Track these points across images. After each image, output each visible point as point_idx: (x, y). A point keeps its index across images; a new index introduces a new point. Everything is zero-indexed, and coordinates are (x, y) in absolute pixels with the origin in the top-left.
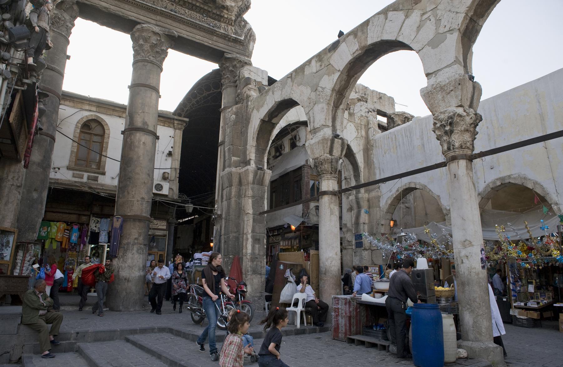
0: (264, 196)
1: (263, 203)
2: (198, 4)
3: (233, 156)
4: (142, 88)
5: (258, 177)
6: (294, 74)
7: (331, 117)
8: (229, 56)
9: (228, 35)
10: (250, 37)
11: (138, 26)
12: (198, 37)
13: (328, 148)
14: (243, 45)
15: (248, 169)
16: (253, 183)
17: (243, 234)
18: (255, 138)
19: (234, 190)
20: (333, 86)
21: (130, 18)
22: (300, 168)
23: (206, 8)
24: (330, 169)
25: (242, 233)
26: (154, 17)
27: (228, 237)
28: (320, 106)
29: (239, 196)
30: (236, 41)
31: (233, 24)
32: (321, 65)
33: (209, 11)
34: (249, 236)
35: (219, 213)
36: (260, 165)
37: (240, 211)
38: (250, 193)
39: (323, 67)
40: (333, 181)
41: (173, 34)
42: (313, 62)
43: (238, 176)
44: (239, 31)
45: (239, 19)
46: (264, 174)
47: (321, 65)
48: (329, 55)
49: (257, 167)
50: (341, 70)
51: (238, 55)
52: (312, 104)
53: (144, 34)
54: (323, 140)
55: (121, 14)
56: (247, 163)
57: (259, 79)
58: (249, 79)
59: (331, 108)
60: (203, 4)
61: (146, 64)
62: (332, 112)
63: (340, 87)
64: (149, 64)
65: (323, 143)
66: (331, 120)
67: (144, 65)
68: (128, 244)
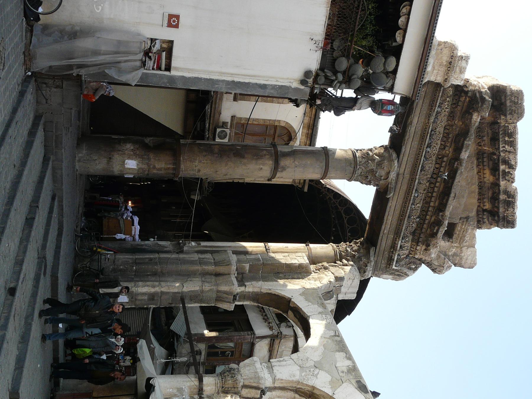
0: (204, 303)
1: (195, 302)
2: (428, 217)
3: (250, 265)
4: (324, 164)
5: (225, 295)
6: (338, 339)
7: (285, 385)
9: (396, 250)
10: (398, 275)
11: (394, 155)
12: (390, 218)
13: (249, 384)
14: (386, 267)
15: (233, 284)
16: (218, 291)
17: (160, 281)
18: (270, 292)
19: (211, 268)
20: (318, 387)
21: (403, 148)
22: (250, 329)
23: (425, 226)
24: (227, 386)
25: (161, 279)
26: (408, 171)
27: (156, 263)
28: (298, 373)
29: (205, 274)
30: (390, 260)
31: (411, 256)
32: (343, 372)
33: (421, 230)
34: (157, 289)
35: (185, 248)
36: (240, 297)
37: (187, 276)
38: (207, 287)
39: (341, 374)
40: (214, 389)
41: (388, 192)
42: (348, 363)
43: (226, 272)
44: (403, 263)
45: (419, 262)
46: (230, 302)
47: (343, 372)
48: (354, 381)
49: (237, 294)
50: (334, 396)
51: (373, 263)
52: (300, 362)
53: (386, 163)
54: (259, 377)
55: (406, 138)
56: (241, 282)
57: (343, 289)
59: (294, 386)
60: (429, 222)
61: (353, 166)
62: (290, 386)
63: (317, 395)
64: (352, 169)
65: (255, 378)
66: (281, 385)
67: (351, 164)
68: (149, 159)
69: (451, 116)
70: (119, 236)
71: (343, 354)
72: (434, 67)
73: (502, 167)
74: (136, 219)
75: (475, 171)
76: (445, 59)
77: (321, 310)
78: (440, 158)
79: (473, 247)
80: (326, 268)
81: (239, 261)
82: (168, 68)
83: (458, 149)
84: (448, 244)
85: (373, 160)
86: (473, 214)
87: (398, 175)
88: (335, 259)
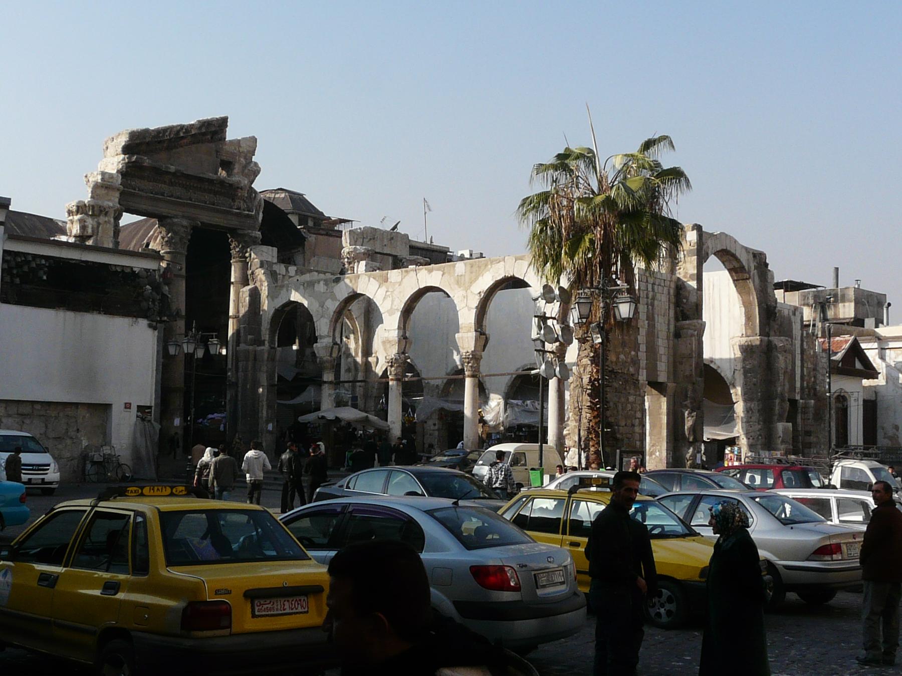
8: (240, 232)
11: (169, 221)
19: (250, 364)
30: (248, 216)
34: (265, 403)
35: (233, 380)
38: (264, 368)
42: (322, 283)
53: (175, 228)
56: (262, 343)
57: (269, 260)
70: (222, 428)
71: (316, 285)
72: (109, 200)
73: (182, 134)
74: (210, 416)
75: (181, 149)
76: (103, 192)
77: (285, 290)
78: (172, 184)
79: (239, 141)
80: (253, 273)
81: (245, 343)
82: (150, 407)
83: (168, 173)
84: (237, 166)
85: (172, 238)
86: (213, 145)
87: (183, 217)
88: (245, 265)
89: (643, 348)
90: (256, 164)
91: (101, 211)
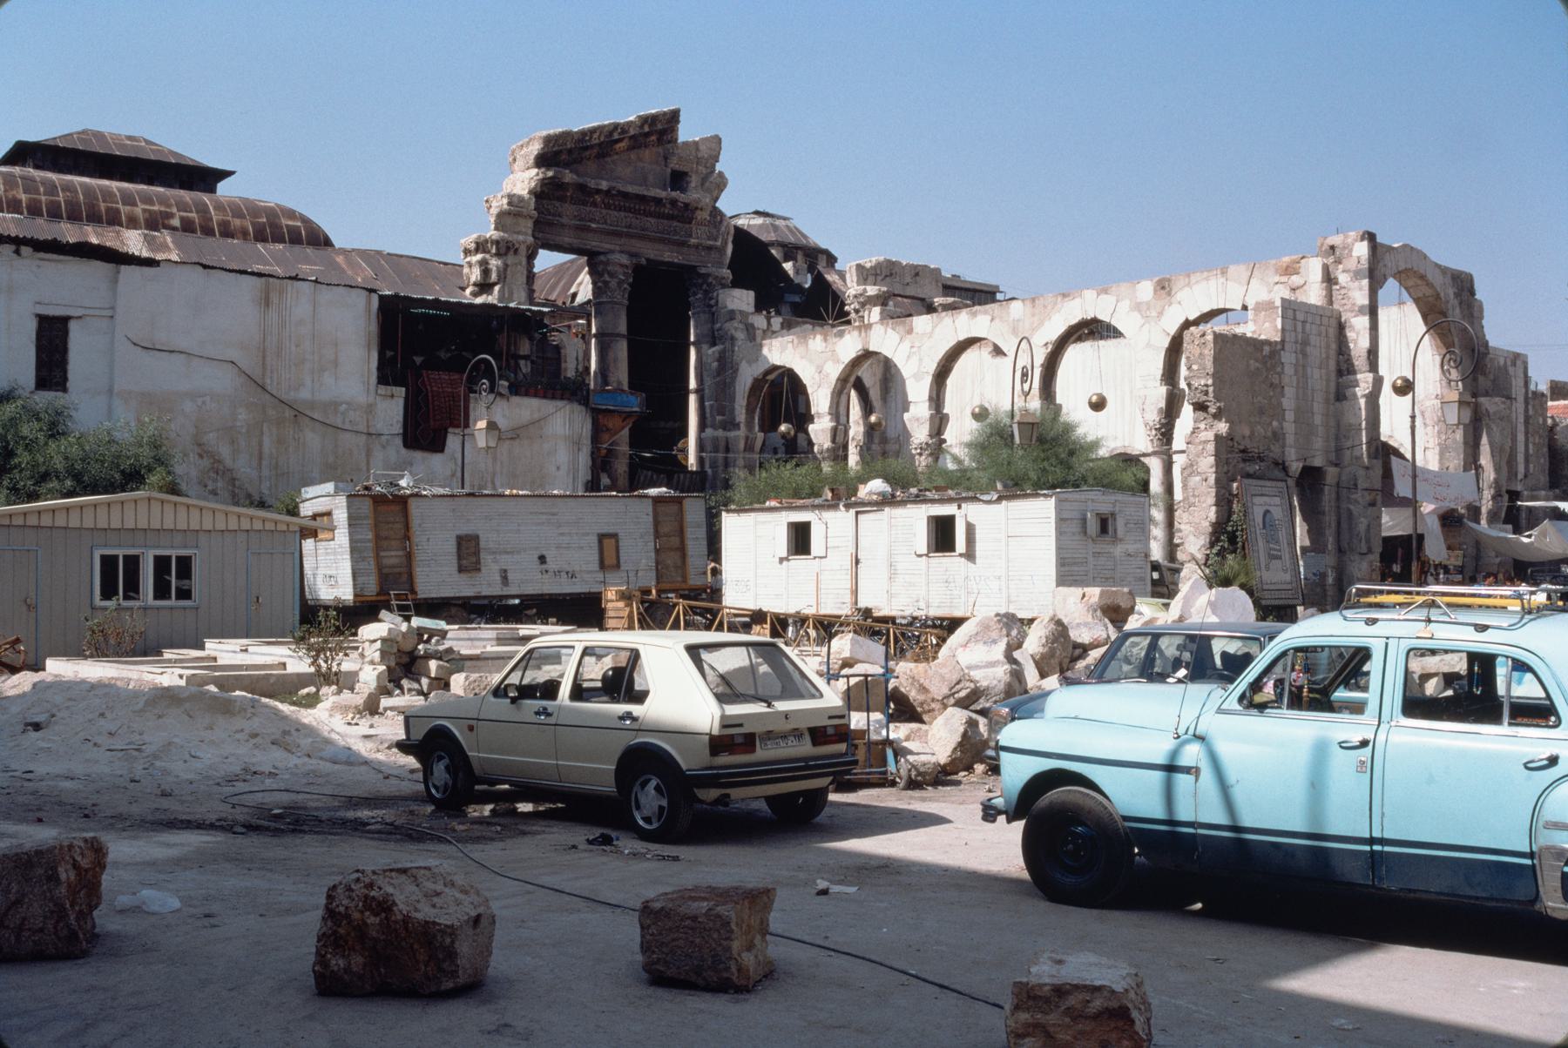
8: (703, 271)
11: (602, 258)
30: (710, 248)
56: (736, 426)
58: (732, 311)
69: (562, 199)
73: (616, 136)
76: (509, 221)
83: (598, 191)
86: (660, 150)
89: (1290, 416)
90: (721, 174)
91: (508, 248)
